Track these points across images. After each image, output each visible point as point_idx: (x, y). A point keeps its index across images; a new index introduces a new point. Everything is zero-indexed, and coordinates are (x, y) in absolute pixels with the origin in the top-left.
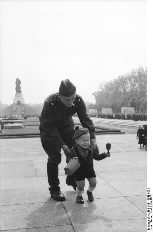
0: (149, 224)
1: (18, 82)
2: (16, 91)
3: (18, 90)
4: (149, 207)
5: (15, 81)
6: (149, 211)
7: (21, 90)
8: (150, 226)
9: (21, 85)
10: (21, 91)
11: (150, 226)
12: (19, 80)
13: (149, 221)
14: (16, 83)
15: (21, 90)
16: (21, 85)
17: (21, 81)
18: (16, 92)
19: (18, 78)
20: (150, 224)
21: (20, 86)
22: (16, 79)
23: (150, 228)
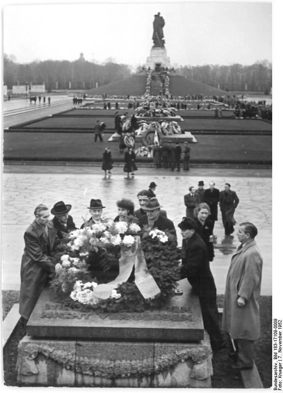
1: (159, 23)
2: (152, 41)
3: (158, 40)
5: (153, 19)
7: (163, 39)
9: (164, 29)
10: (163, 42)
12: (162, 18)
14: (155, 23)
15: (163, 39)
16: (165, 30)
17: (165, 21)
18: (153, 44)
19: (159, 13)
22: (155, 16)
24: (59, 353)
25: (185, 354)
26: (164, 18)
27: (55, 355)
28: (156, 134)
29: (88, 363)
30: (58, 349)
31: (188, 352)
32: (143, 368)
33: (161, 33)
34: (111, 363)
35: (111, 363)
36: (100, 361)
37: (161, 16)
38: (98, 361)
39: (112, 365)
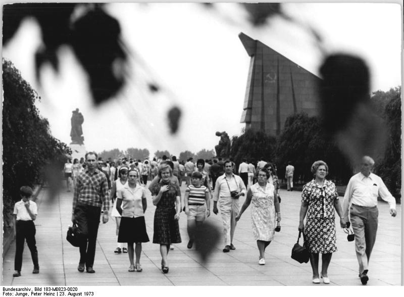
0: (14, 290)
2: (70, 138)
4: (43, 289)
5: (71, 115)
6: (36, 289)
7: (82, 136)
8: (10, 292)
9: (83, 125)
10: (82, 139)
11: (10, 292)
12: (80, 114)
13: (20, 290)
16: (84, 126)
18: (71, 141)
19: (77, 110)
20: (14, 293)
21: (81, 128)
22: (74, 112)
23: (7, 292)
26: (83, 114)
33: (79, 129)
37: (79, 112)
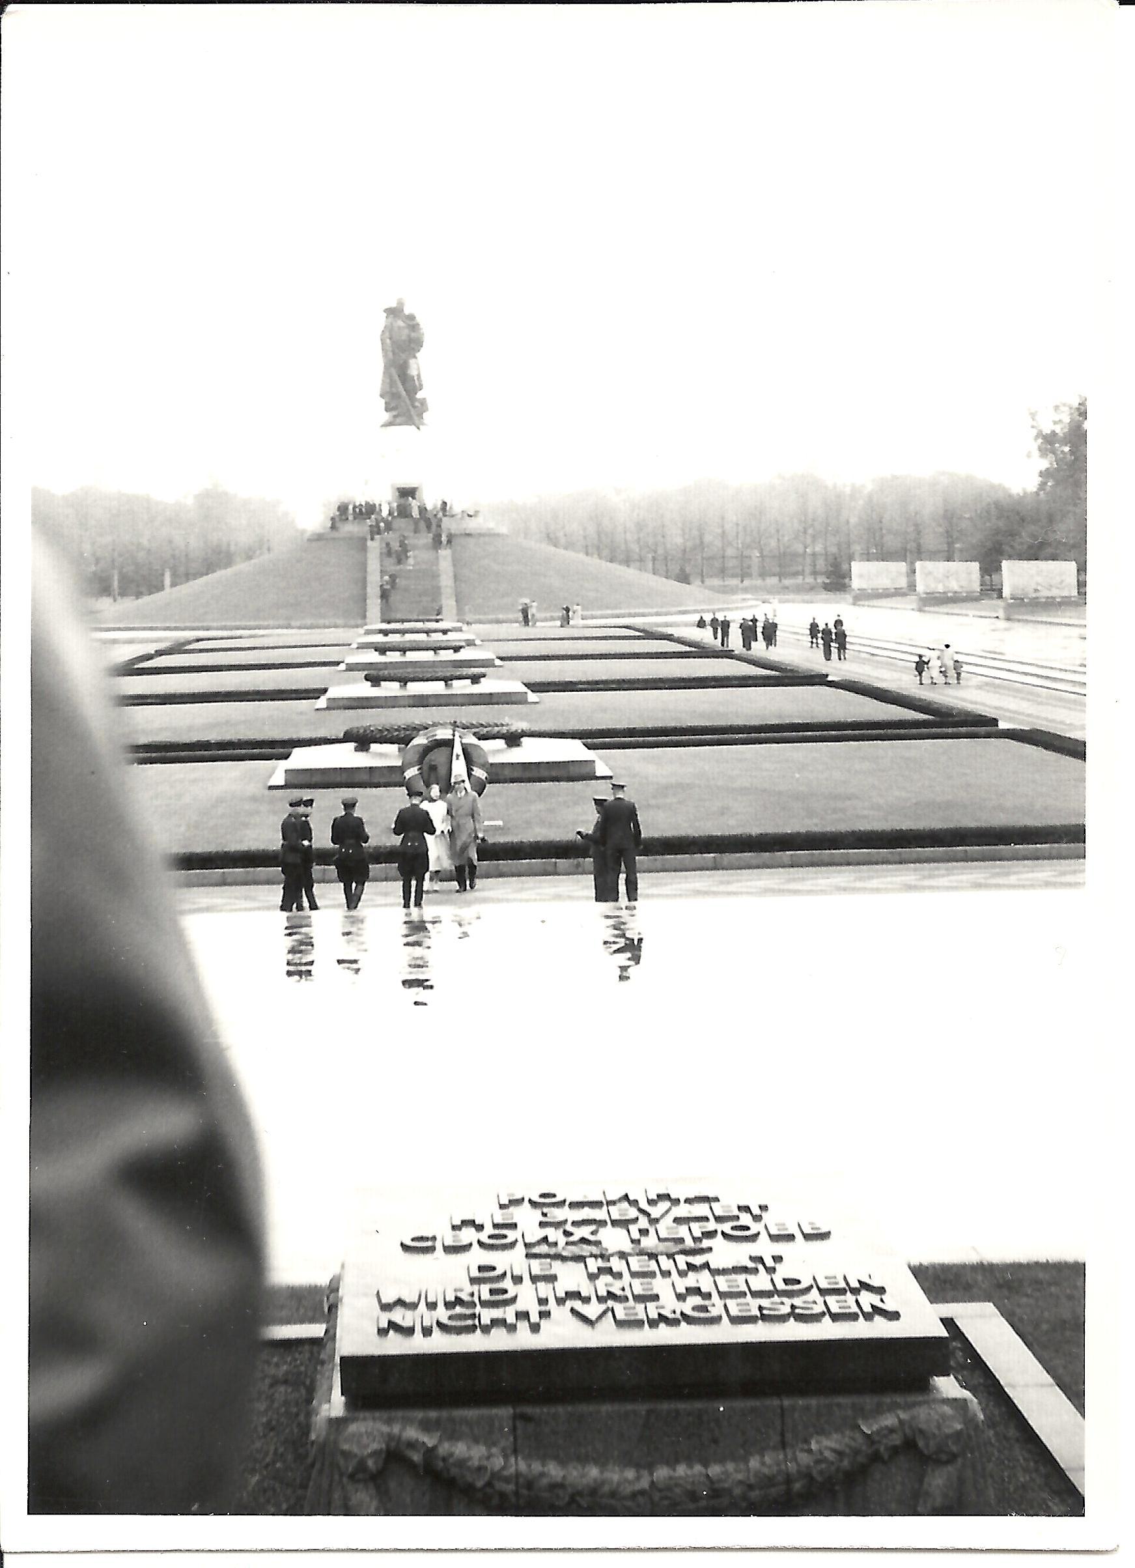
3: (403, 399)
5: (381, 321)
24: (460, 1449)
25: (891, 1430)
27: (444, 1459)
28: (458, 749)
29: (559, 1480)
30: (453, 1436)
31: (901, 1422)
32: (751, 1487)
34: (638, 1478)
35: (638, 1478)
36: (602, 1472)
38: (594, 1472)
39: (644, 1484)
